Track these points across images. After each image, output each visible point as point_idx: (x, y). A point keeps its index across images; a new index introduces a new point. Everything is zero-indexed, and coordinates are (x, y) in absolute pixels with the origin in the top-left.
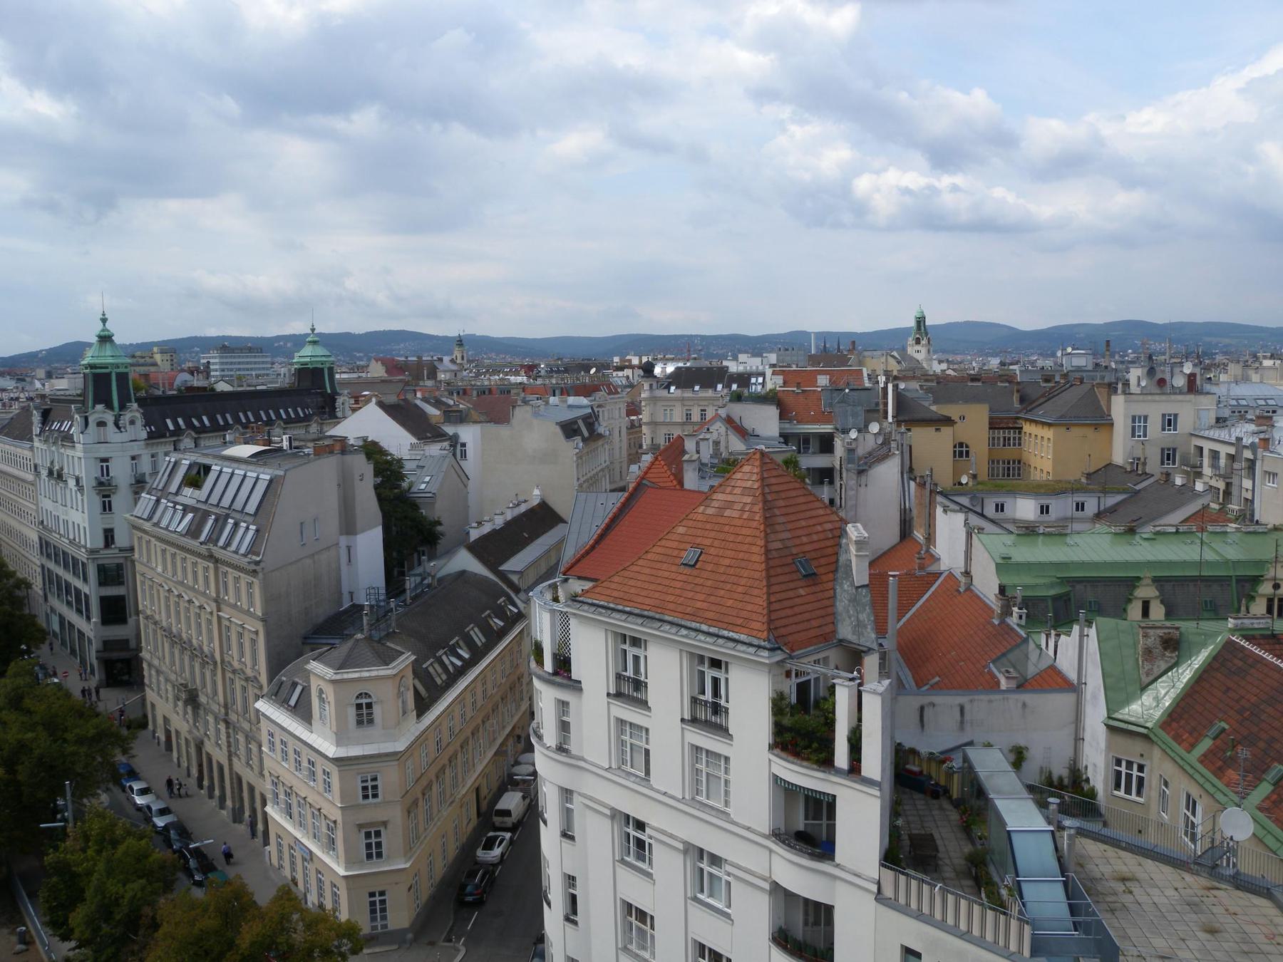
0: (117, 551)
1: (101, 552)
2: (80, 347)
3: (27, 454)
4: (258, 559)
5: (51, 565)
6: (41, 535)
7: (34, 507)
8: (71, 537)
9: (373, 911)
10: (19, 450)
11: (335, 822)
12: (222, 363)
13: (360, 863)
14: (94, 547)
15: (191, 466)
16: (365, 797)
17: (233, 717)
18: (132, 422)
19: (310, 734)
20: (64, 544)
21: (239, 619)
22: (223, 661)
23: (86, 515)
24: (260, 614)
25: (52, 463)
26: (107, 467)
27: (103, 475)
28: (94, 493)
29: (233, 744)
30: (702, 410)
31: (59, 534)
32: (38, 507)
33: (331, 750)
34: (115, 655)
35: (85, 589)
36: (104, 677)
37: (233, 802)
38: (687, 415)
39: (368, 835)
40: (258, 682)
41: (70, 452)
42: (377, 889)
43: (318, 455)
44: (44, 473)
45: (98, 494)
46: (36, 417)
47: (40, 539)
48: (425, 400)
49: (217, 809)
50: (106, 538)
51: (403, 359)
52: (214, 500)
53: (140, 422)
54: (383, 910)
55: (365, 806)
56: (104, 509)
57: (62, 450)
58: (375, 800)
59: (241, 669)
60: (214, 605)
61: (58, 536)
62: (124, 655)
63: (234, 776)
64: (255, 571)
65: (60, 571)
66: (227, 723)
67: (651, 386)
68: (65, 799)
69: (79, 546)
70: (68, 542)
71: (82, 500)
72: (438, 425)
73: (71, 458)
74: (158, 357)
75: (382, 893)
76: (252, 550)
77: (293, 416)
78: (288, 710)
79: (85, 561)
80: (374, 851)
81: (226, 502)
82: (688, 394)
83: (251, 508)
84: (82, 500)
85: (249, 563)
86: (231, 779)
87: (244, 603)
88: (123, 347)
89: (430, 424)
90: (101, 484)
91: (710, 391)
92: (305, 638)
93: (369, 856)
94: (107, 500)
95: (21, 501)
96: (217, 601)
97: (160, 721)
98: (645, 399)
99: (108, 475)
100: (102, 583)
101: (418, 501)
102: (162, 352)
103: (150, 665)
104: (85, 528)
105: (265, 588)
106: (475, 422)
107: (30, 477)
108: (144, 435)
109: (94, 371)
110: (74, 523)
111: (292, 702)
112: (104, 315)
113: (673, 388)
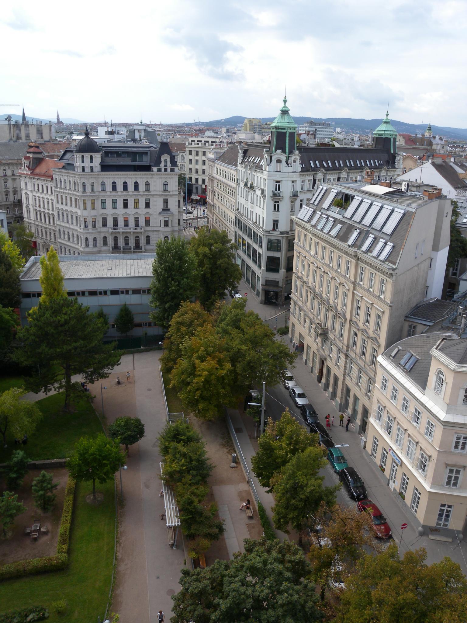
0: (279, 233)
3: (233, 172)
4: (394, 267)
5: (241, 233)
7: (234, 201)
8: (254, 221)
9: (440, 515)
10: (229, 170)
11: (430, 457)
13: (441, 487)
14: (267, 229)
15: (338, 194)
16: (456, 448)
17: (352, 354)
18: (295, 162)
19: (423, 395)
20: (250, 224)
21: (361, 294)
22: (351, 320)
23: (265, 211)
24: (389, 302)
25: (247, 179)
26: (279, 185)
27: (276, 190)
28: (270, 199)
29: (348, 369)
31: (247, 217)
32: (236, 201)
33: (442, 415)
34: (271, 289)
35: (259, 250)
36: (263, 299)
37: (341, 400)
39: (451, 471)
40: (378, 342)
41: (259, 175)
42: (447, 504)
43: (431, 199)
44: (242, 184)
45: (273, 200)
46: (240, 154)
47: (236, 218)
48: (455, 163)
49: (329, 399)
50: (274, 224)
51: (414, 135)
52: (357, 218)
53: (298, 162)
54: (447, 516)
56: (275, 209)
57: (254, 174)
58: (462, 451)
59: (365, 330)
60: (351, 286)
61: (247, 219)
62: (275, 289)
63: (345, 386)
64: (391, 274)
65: (246, 237)
66: (347, 356)
68: (260, 391)
69: (258, 227)
70: (252, 223)
71: (264, 203)
72: (464, 180)
73: (259, 178)
75: (450, 506)
76: (388, 259)
77: (373, 165)
78: (403, 371)
79: (262, 236)
80: (452, 481)
81: (367, 221)
83: (389, 228)
84: (264, 203)
85: (389, 269)
86: (343, 387)
87: (376, 289)
88: (294, 118)
89: (459, 179)
90: (275, 195)
92: (407, 317)
93: (448, 483)
94: (277, 204)
95: (226, 196)
96: (354, 284)
97: (297, 335)
99: (279, 190)
101: (461, 229)
103: (295, 303)
104: (263, 218)
105: (395, 285)
107: (234, 185)
108: (299, 169)
109: (278, 130)
110: (257, 214)
111: (393, 354)
112: (285, 98)
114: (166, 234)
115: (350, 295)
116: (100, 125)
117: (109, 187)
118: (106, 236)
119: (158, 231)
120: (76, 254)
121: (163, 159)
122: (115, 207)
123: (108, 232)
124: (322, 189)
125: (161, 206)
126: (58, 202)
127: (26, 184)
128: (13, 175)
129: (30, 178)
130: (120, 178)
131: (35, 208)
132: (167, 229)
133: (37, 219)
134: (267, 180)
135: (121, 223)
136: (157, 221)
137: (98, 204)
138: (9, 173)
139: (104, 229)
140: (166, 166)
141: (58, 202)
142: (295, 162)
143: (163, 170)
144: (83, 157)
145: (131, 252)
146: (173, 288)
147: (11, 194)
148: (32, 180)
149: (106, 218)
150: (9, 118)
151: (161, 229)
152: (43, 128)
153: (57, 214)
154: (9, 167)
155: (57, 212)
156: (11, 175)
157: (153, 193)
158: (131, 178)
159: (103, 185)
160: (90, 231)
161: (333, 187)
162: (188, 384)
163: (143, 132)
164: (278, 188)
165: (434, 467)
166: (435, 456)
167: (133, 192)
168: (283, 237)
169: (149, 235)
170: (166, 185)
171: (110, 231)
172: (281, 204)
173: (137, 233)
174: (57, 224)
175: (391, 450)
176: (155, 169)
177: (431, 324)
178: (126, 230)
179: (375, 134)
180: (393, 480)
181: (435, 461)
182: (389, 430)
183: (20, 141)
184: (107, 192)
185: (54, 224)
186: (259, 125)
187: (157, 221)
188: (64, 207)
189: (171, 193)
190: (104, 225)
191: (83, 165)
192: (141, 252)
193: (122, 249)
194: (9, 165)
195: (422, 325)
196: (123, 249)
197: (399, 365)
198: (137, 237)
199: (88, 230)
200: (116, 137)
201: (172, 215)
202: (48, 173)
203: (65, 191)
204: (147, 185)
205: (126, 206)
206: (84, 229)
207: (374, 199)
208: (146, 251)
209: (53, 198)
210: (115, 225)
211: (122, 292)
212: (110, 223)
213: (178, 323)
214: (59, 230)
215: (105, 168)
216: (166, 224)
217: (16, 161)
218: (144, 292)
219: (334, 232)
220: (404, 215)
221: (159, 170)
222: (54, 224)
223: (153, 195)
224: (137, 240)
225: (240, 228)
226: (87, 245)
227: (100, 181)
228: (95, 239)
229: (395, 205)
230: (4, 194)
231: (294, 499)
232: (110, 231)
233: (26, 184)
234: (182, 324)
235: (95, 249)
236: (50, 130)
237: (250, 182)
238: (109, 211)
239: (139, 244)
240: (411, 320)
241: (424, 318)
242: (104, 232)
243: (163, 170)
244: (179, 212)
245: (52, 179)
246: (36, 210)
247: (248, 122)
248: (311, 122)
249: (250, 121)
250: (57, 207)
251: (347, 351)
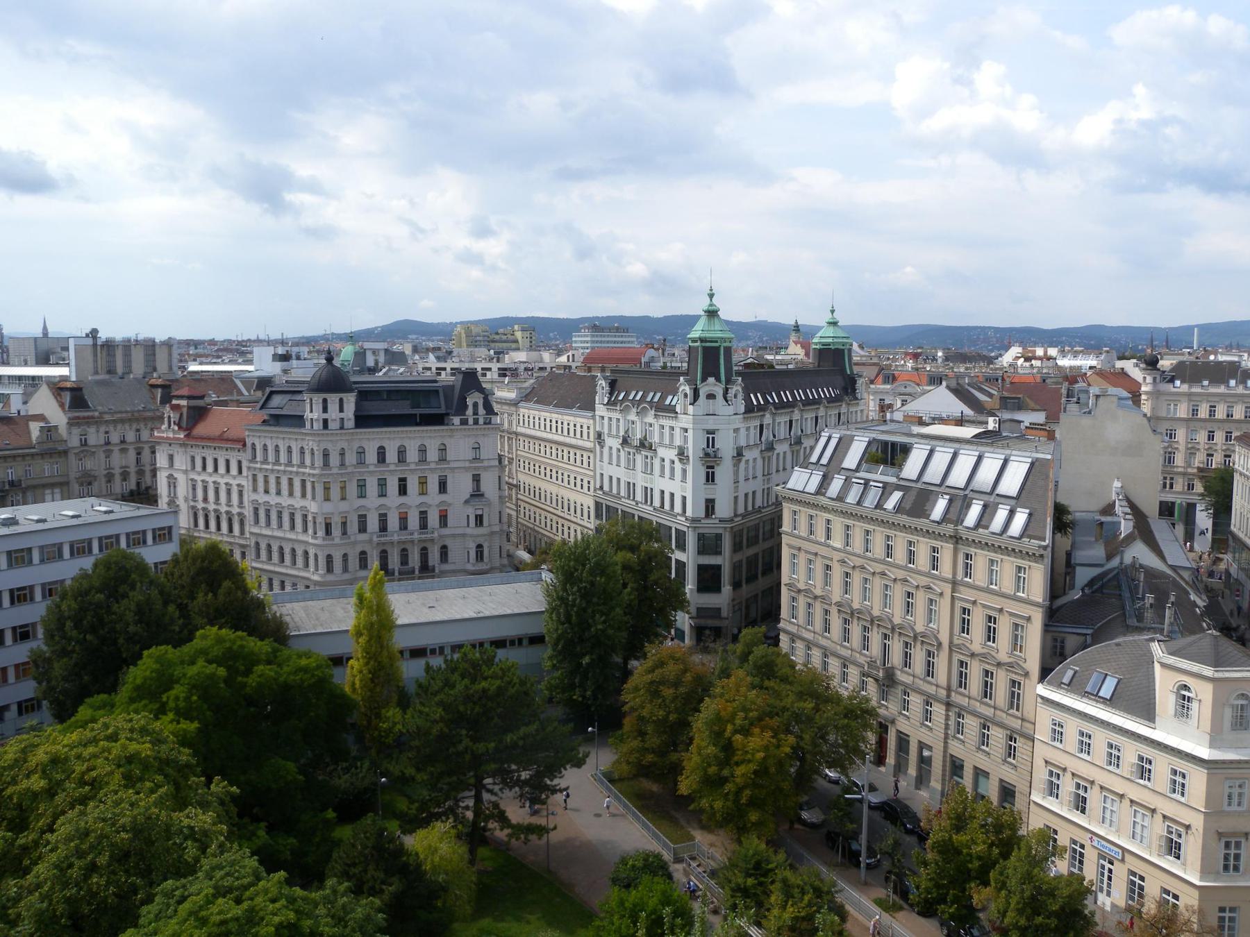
0: (717, 521)
1: (679, 518)
2: (692, 320)
3: (586, 422)
4: (1043, 543)
6: (598, 500)
7: (592, 473)
11: (1188, 827)
12: (593, 342)
14: (695, 516)
15: (870, 443)
18: (735, 396)
22: (951, 642)
24: (1041, 600)
25: (626, 432)
26: (713, 438)
27: (708, 447)
28: (699, 464)
30: (1211, 406)
38: (1193, 410)
41: (667, 423)
44: (613, 443)
45: (703, 465)
50: (707, 507)
55: (1229, 814)
56: (708, 480)
60: (947, 589)
64: (1042, 556)
66: (949, 705)
67: (1155, 379)
74: (519, 335)
82: (1196, 389)
88: (728, 323)
90: (707, 455)
91: (1223, 387)
94: (710, 470)
96: (955, 584)
98: (1146, 393)
99: (713, 446)
100: (702, 551)
102: (523, 330)
104: (684, 498)
106: (1033, 410)
109: (704, 344)
113: (1178, 383)
114: (480, 541)
115: (945, 603)
116: (259, 342)
117: (372, 457)
118: (365, 549)
119: (464, 535)
120: (288, 589)
121: (470, 401)
122: (383, 494)
123: (370, 541)
124: (830, 438)
125: (466, 486)
126: (255, 490)
127: (171, 458)
128: (123, 442)
129: (183, 445)
130: (391, 439)
131: (192, 503)
132: (480, 531)
133: (196, 525)
134: (690, 432)
135: (393, 523)
136: (460, 515)
137: (352, 489)
138: (115, 438)
139: (363, 537)
140: (475, 413)
141: (255, 490)
142: (735, 396)
143: (471, 421)
144: (325, 401)
145: (413, 579)
146: (600, 627)
147: (118, 478)
148: (189, 449)
149: (365, 516)
151: (469, 531)
152: (157, 349)
153: (252, 513)
154: (115, 426)
155: (251, 509)
156: (118, 441)
157: (452, 465)
158: (412, 439)
159: (361, 452)
160: (337, 541)
161: (854, 433)
162: (725, 780)
163: (382, 354)
164: (711, 443)
165: (1200, 841)
166: (1197, 822)
167: (417, 464)
168: (725, 528)
169: (446, 543)
170: (477, 448)
171: (375, 539)
172: (719, 472)
173: (424, 541)
174: (251, 533)
175: (1094, 838)
177: (1089, 631)
178: (404, 536)
179: (816, 344)
180: (1105, 892)
181: (1201, 831)
182: (1080, 804)
183: (132, 376)
184: (368, 466)
185: (242, 532)
186: (484, 336)
187: (460, 515)
188: (273, 499)
189: (486, 464)
190: (363, 528)
191: (342, 415)
192: (433, 577)
193: (397, 574)
194: (115, 422)
195: (1075, 636)
196: (400, 574)
197: (1086, 694)
198: (404, 550)
199: (333, 539)
201: (489, 504)
202: (233, 434)
203: (276, 467)
204: (443, 449)
205: (403, 490)
206: (324, 539)
207: (957, 445)
208: (443, 574)
209: (244, 483)
210: (383, 528)
211: (512, 643)
212: (373, 524)
213: (652, 682)
214: (257, 544)
215: (363, 420)
216: (479, 520)
217: (130, 415)
218: (512, 643)
219: (890, 504)
220: (1032, 464)
221: (464, 422)
222: (242, 532)
223: (453, 469)
224: (424, 553)
226: (330, 569)
227: (356, 445)
228: (345, 556)
229: (1008, 452)
230: (104, 480)
231: (1039, 915)
232: (375, 539)
233: (171, 458)
234: (662, 682)
235: (347, 576)
236: (170, 355)
238: (372, 501)
239: (427, 561)
240: (1059, 629)
241: (1075, 623)
242: (361, 542)
243: (471, 421)
244: (500, 497)
245: (244, 445)
246: (193, 507)
247: (463, 331)
248: (595, 325)
249: (467, 326)
250: (251, 499)
251: (948, 696)
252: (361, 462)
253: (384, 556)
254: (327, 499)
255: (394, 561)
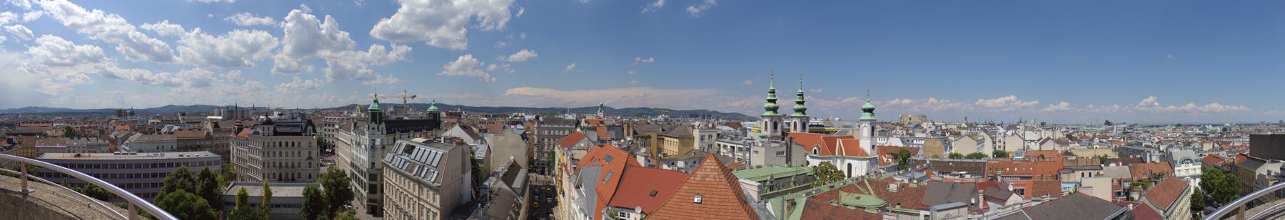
20: (359, 165)
44: (354, 142)
65: (357, 173)
117: (277, 144)
122: (281, 156)
130: (284, 139)
136: (305, 164)
137: (271, 154)
150: (228, 107)
159: (274, 143)
176: (304, 134)
200: (283, 117)
204: (299, 143)
208: (298, 182)
221: (306, 135)
225: (353, 167)
237: (358, 141)
252: (274, 146)
253: (280, 175)
254: (264, 156)
255: (283, 176)
